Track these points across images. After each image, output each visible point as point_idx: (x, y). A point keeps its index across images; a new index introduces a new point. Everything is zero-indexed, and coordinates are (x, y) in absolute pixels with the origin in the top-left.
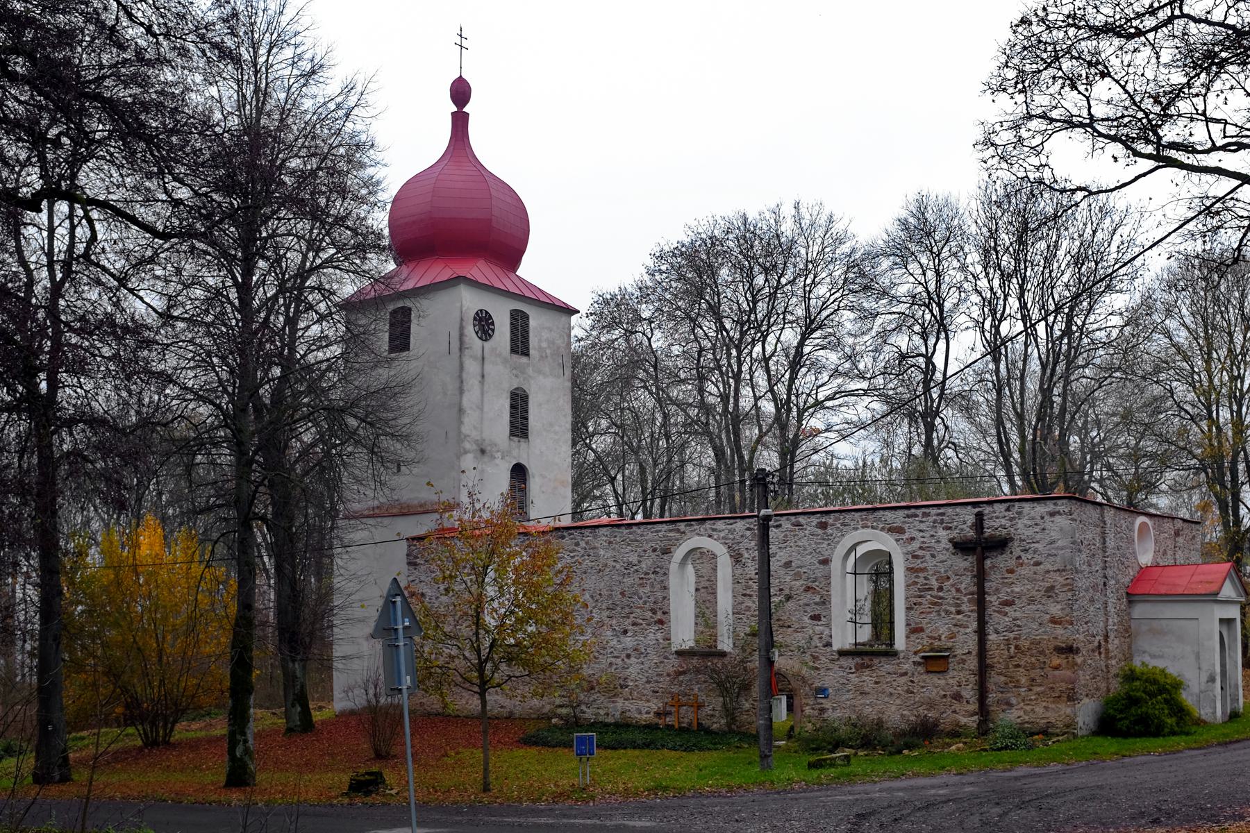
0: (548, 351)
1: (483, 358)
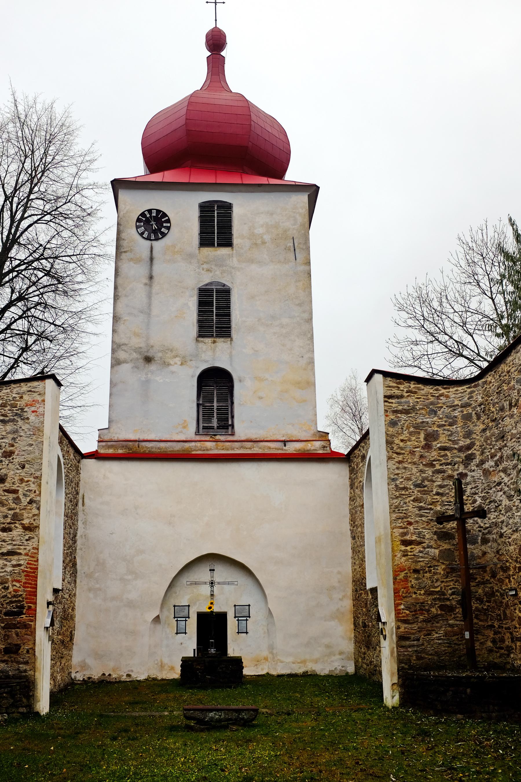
0: (267, 237)
1: (152, 259)
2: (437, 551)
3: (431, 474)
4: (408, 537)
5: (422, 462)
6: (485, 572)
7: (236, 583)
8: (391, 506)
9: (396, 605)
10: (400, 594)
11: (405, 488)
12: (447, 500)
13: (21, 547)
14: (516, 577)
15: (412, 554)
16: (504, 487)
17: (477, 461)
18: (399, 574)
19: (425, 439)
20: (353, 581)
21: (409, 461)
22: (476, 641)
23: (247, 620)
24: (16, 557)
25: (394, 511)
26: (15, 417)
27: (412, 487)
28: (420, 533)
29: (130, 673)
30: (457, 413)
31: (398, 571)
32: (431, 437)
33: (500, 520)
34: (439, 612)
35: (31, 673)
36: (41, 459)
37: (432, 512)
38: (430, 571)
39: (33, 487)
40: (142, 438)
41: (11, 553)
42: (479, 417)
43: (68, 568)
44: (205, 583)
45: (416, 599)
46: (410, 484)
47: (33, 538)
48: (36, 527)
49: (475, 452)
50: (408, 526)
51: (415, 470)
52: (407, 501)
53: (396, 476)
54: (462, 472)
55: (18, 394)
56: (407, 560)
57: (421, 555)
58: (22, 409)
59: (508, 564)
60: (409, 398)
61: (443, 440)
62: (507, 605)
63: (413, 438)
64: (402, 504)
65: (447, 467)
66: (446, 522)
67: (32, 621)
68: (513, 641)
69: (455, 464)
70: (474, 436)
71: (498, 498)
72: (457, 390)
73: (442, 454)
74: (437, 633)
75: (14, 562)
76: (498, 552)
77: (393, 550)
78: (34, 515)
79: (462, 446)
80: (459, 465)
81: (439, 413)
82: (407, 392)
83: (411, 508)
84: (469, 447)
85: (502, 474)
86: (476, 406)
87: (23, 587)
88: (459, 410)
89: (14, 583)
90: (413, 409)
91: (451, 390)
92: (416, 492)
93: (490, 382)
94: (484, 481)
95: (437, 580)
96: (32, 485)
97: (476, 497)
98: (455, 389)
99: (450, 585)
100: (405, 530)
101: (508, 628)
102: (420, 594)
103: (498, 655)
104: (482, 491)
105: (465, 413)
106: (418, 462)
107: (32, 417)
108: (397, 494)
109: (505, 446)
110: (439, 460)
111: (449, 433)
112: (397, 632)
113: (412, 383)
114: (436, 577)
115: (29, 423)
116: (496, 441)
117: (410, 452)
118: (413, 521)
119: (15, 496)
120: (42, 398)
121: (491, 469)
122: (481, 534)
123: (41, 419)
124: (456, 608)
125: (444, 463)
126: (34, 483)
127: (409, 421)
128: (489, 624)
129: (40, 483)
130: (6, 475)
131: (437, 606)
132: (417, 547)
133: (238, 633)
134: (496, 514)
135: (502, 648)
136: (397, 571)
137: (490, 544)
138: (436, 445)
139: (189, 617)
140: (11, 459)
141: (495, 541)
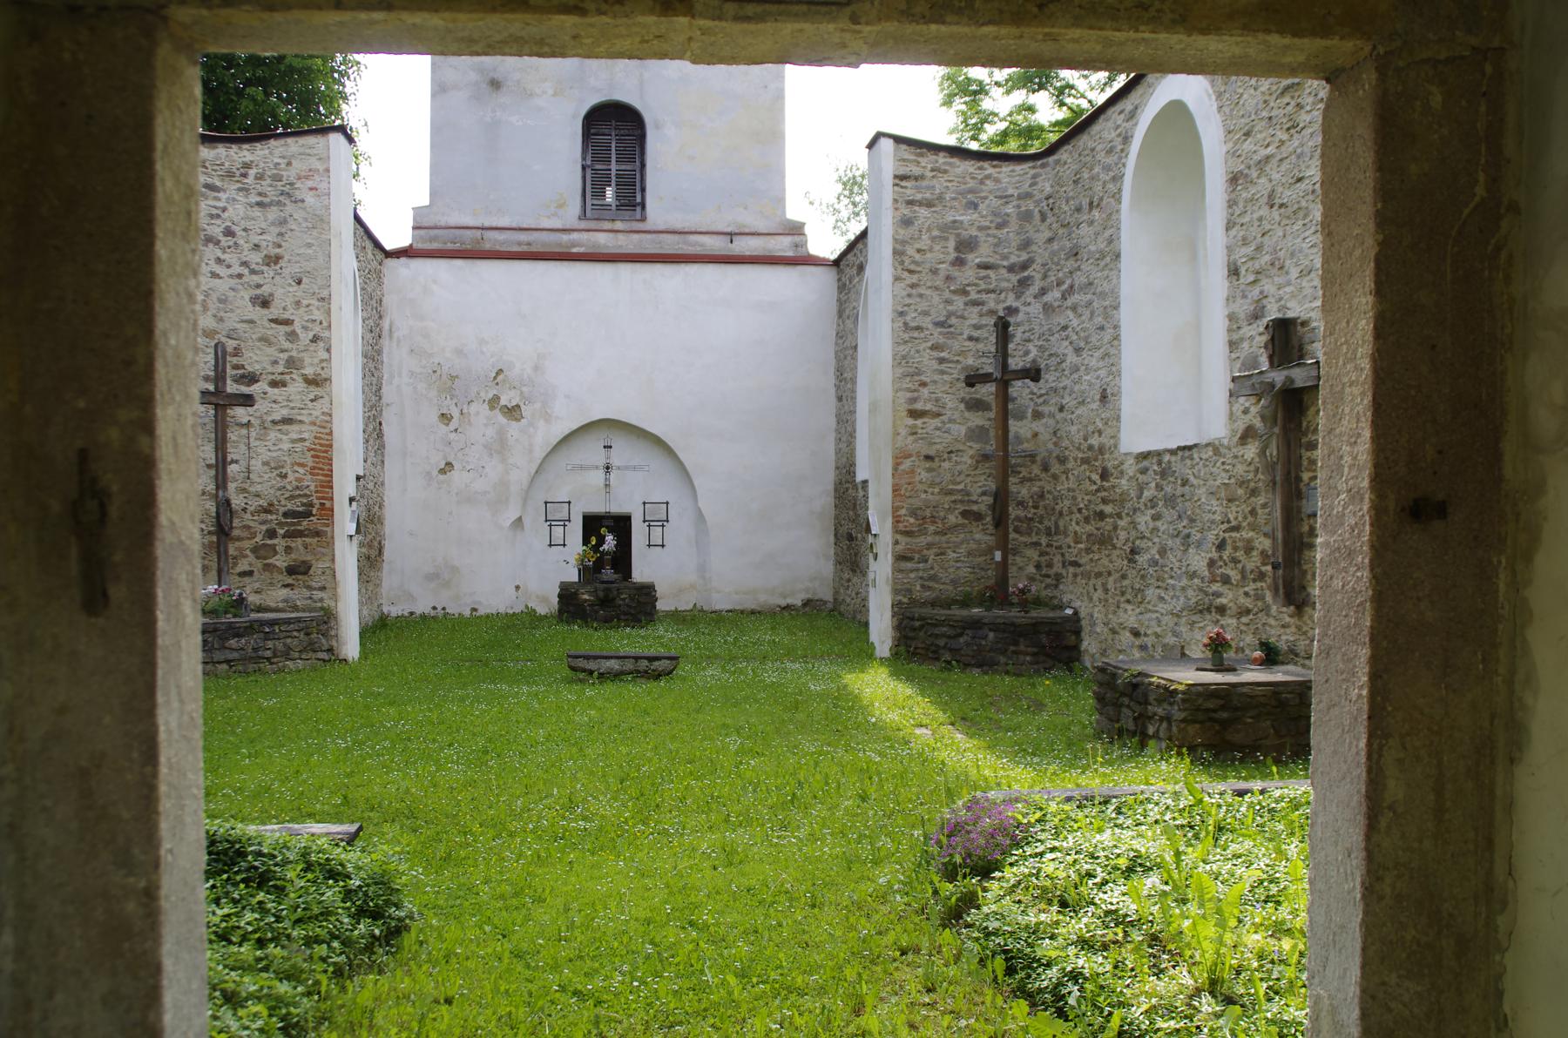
2: (963, 430)
3: (962, 307)
4: (919, 406)
6: (1033, 462)
7: (647, 468)
8: (894, 356)
9: (895, 509)
10: (902, 492)
11: (918, 328)
13: (303, 411)
14: (1076, 472)
15: (924, 431)
16: (1071, 334)
17: (1034, 289)
18: (901, 463)
19: (957, 249)
20: (837, 468)
21: (929, 284)
22: (1012, 564)
23: (663, 526)
24: (295, 427)
26: (281, 198)
27: (930, 326)
28: (937, 400)
29: (476, 607)
30: (1010, 209)
32: (966, 246)
33: (1061, 385)
35: (332, 604)
36: (329, 268)
37: (959, 366)
38: (950, 459)
39: (317, 315)
40: (487, 224)
41: (287, 421)
42: (1043, 219)
43: (371, 441)
44: (597, 467)
45: (925, 500)
46: (926, 322)
47: (322, 397)
48: (326, 380)
51: (936, 299)
52: (921, 348)
53: (906, 308)
55: (283, 157)
56: (916, 441)
57: (938, 433)
58: (291, 184)
59: (1067, 453)
60: (935, 180)
61: (984, 253)
62: (1061, 514)
63: (937, 248)
64: (912, 353)
66: (980, 383)
67: (327, 525)
68: (1064, 566)
71: (1060, 351)
72: (1013, 171)
73: (981, 275)
74: (954, 552)
75: (295, 436)
76: (1055, 433)
78: (322, 361)
81: (982, 206)
82: (932, 170)
83: (927, 360)
84: (1024, 266)
85: (1070, 314)
86: (1040, 200)
87: (311, 474)
88: (1015, 203)
89: (296, 468)
90: (940, 198)
91: (1004, 169)
92: (936, 335)
93: (1065, 163)
95: (960, 473)
96: (316, 312)
97: (1031, 346)
98: (1011, 168)
100: (916, 394)
101: (1059, 547)
102: (932, 494)
103: (1043, 585)
104: (1039, 338)
105: (1023, 209)
107: (310, 199)
108: (906, 336)
109: (1079, 269)
110: (976, 285)
111: (996, 240)
113: (942, 154)
114: (958, 468)
115: (304, 209)
116: (1067, 259)
117: (931, 270)
118: (928, 380)
119: (288, 329)
120: (325, 166)
121: (1056, 304)
122: (1032, 403)
123: (326, 202)
124: (986, 515)
125: (984, 290)
126: (318, 309)
127: (932, 220)
128: (1034, 540)
129: (329, 308)
130: (271, 295)
131: (957, 512)
133: (649, 546)
134: (1057, 374)
135: (1048, 576)
136: (900, 457)
137: (1045, 420)
138: (973, 259)
139: (569, 521)
140: (278, 267)
141: (1052, 415)
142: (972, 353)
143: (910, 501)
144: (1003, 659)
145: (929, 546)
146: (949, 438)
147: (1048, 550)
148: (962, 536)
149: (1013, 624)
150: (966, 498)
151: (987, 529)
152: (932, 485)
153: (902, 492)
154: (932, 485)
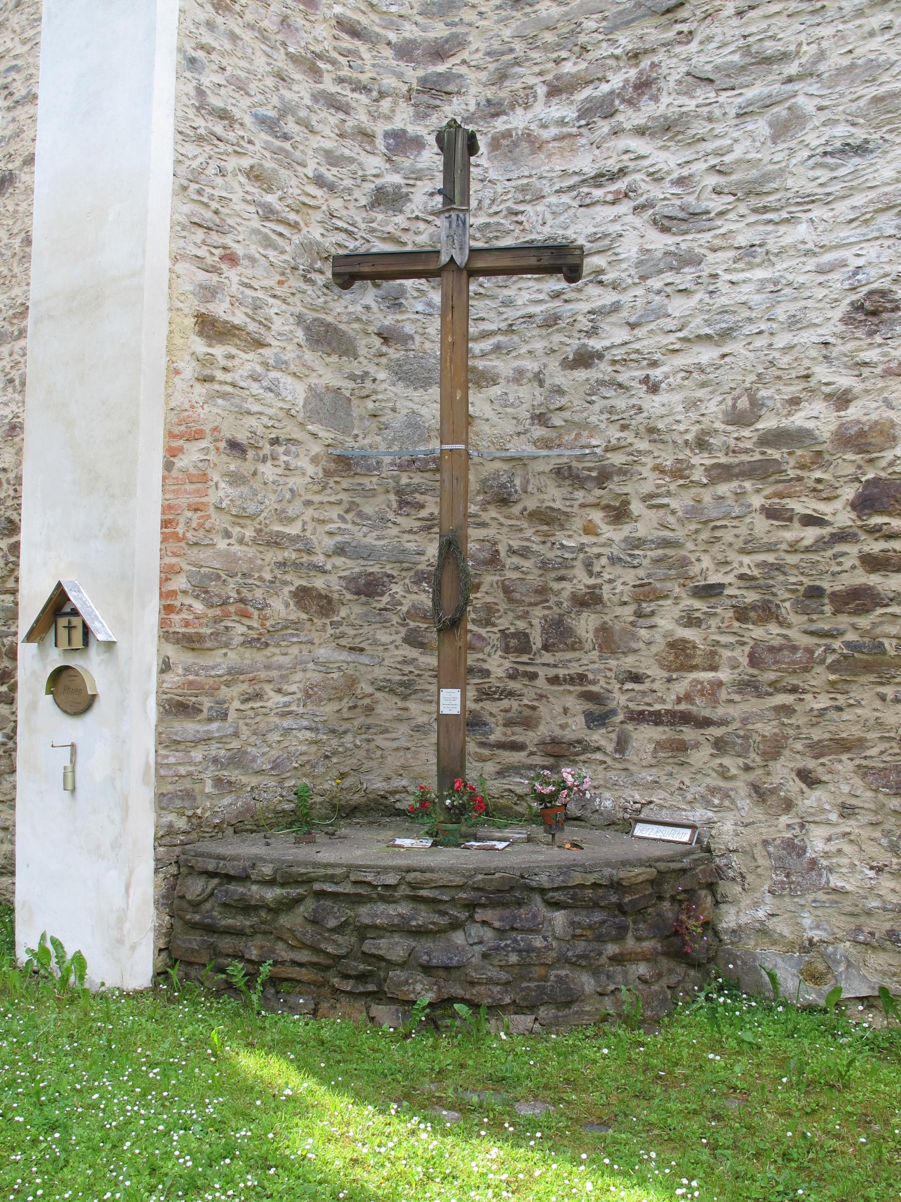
3: (308, 101)
4: (220, 309)
5: (284, 44)
9: (168, 573)
10: (180, 530)
11: (223, 115)
12: (344, 213)
15: (228, 377)
18: (181, 450)
21: (249, 17)
25: (185, 188)
27: (248, 120)
28: (257, 306)
31: (180, 436)
34: (293, 617)
37: (296, 239)
45: (229, 557)
46: (241, 107)
49: (463, 70)
50: (224, 267)
51: (260, 62)
53: (200, 54)
54: (404, 132)
57: (255, 388)
64: (211, 170)
65: (356, 95)
69: (382, 95)
70: (468, 15)
73: (345, 45)
74: (279, 691)
77: (170, 350)
79: (413, 42)
80: (396, 103)
84: (439, 52)
94: (492, 175)
99: (332, 521)
100: (215, 278)
102: (241, 541)
106: (273, 37)
110: (333, 62)
112: (160, 684)
118: (240, 250)
131: (286, 590)
132: (242, 355)
137: (495, 391)
142: (318, 216)
143: (194, 554)
144: (587, 982)
145: (235, 674)
146: (274, 407)
147: (513, 685)
148: (294, 650)
149: (616, 886)
150: (306, 558)
151: (343, 635)
152: (241, 518)
153: (180, 530)
154: (241, 518)
